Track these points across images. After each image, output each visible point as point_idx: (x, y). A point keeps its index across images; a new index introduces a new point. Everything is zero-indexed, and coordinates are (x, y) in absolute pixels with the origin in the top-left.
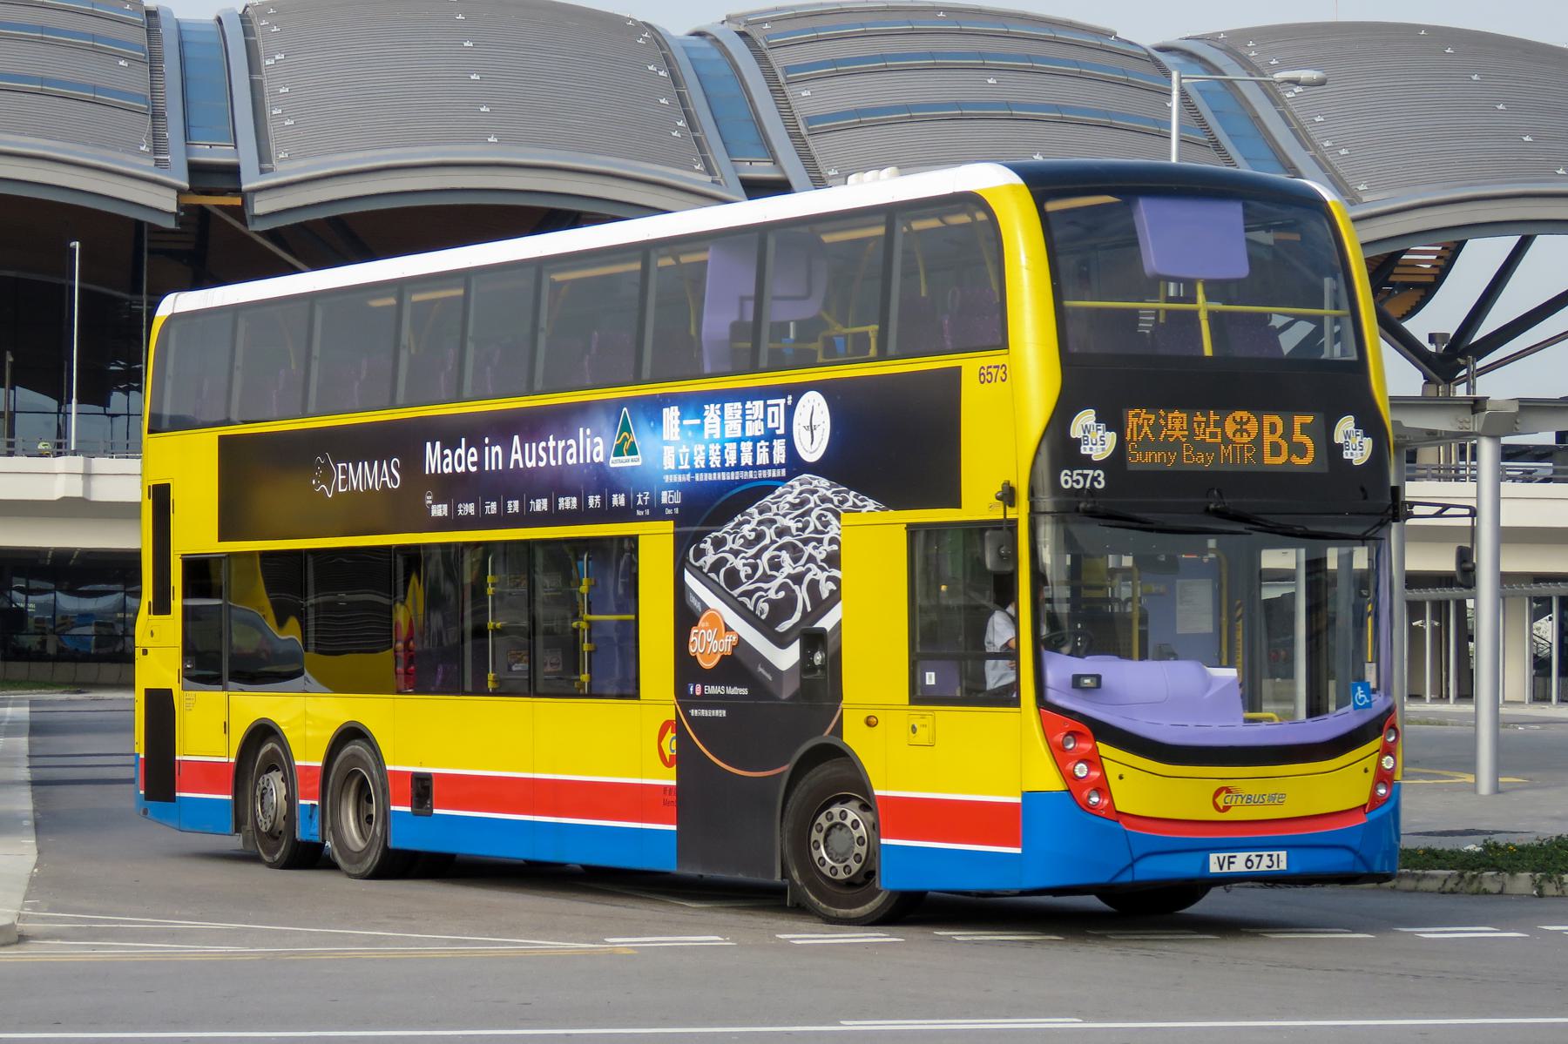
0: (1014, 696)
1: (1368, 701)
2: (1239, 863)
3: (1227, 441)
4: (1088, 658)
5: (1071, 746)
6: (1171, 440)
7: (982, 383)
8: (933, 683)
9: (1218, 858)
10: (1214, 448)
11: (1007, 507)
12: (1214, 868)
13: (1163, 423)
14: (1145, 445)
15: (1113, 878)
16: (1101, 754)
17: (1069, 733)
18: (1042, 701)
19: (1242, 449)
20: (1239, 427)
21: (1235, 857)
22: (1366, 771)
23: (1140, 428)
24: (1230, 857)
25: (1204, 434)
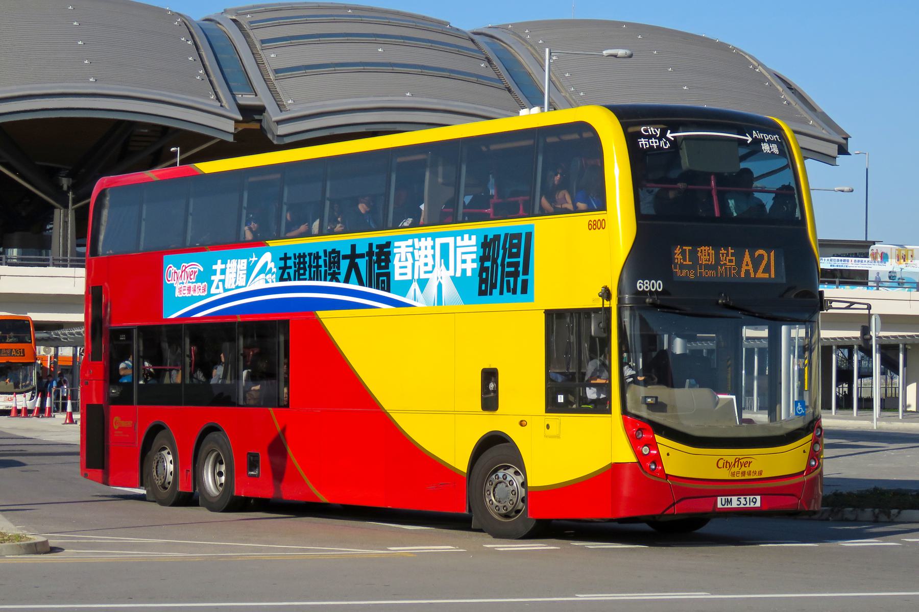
0: (608, 407)
1: (803, 412)
2: (735, 502)
4: (649, 387)
5: (640, 436)
7: (590, 229)
8: (562, 401)
11: (605, 300)
15: (664, 511)
17: (639, 429)
18: (624, 411)
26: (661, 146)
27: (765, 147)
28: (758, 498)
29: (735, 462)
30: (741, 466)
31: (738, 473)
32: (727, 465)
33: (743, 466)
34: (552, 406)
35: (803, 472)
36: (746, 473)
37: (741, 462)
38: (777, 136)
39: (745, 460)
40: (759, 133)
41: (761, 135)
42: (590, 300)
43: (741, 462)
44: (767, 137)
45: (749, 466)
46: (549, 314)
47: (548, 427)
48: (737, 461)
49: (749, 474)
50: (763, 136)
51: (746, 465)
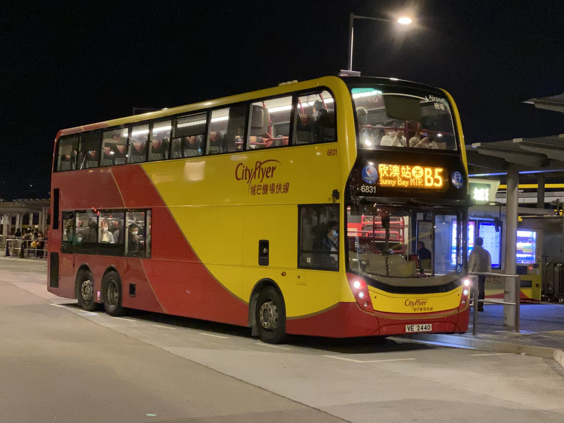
2: (415, 328)
3: (413, 177)
6: (394, 176)
9: (408, 326)
10: (408, 180)
12: (407, 331)
13: (391, 170)
14: (385, 178)
16: (369, 289)
18: (348, 270)
19: (418, 180)
20: (417, 172)
21: (413, 326)
22: (459, 295)
23: (383, 171)
24: (412, 326)
25: (405, 174)
26: (373, 101)
27: (436, 106)
28: (431, 325)
29: (416, 302)
30: (420, 305)
31: (418, 309)
32: (411, 303)
33: (421, 304)
34: (301, 265)
35: (458, 308)
36: (423, 309)
37: (420, 302)
38: (444, 99)
39: (422, 301)
40: (433, 96)
41: (434, 98)
42: (325, 198)
43: (420, 302)
44: (437, 99)
45: (425, 305)
46: (300, 207)
47: (299, 277)
48: (418, 301)
49: (425, 309)
50: (435, 98)
51: (423, 304)
